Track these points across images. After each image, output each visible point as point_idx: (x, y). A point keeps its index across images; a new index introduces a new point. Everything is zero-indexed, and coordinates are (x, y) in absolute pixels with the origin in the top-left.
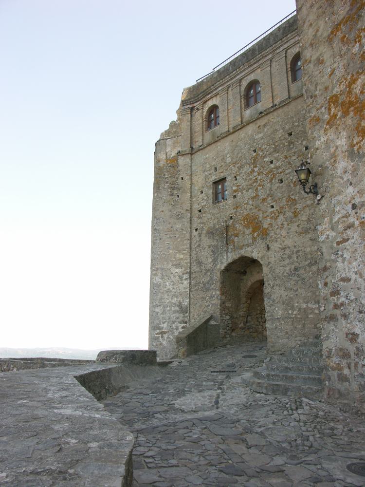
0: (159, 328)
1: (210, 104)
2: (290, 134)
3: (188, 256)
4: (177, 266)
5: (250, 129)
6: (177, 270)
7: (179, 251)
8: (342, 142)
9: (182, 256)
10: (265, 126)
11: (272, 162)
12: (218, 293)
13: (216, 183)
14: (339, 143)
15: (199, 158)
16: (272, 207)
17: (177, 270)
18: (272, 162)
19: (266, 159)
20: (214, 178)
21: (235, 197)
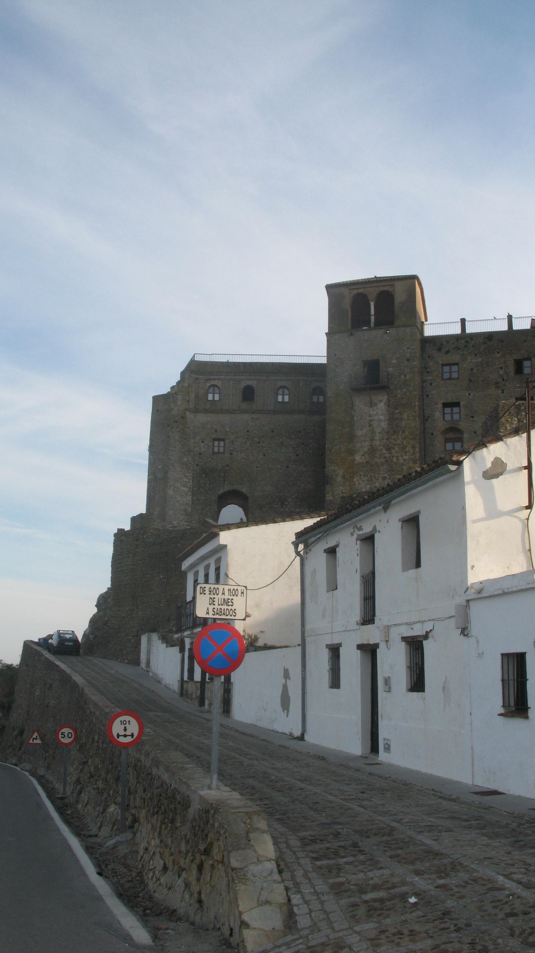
0: (171, 524)
1: (213, 383)
2: (273, 432)
3: (191, 481)
4: (184, 486)
5: (246, 417)
6: (184, 489)
7: (186, 476)
8: (341, 472)
9: (187, 480)
10: (257, 419)
11: (259, 443)
12: (216, 507)
13: (215, 440)
14: (339, 472)
15: (202, 418)
16: (257, 467)
17: (184, 489)
18: (259, 443)
19: (256, 439)
20: (214, 436)
21: (231, 454)
